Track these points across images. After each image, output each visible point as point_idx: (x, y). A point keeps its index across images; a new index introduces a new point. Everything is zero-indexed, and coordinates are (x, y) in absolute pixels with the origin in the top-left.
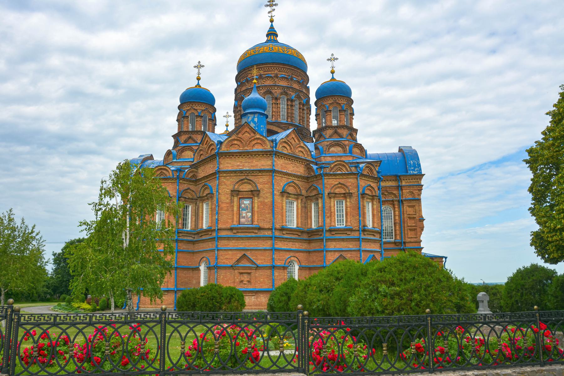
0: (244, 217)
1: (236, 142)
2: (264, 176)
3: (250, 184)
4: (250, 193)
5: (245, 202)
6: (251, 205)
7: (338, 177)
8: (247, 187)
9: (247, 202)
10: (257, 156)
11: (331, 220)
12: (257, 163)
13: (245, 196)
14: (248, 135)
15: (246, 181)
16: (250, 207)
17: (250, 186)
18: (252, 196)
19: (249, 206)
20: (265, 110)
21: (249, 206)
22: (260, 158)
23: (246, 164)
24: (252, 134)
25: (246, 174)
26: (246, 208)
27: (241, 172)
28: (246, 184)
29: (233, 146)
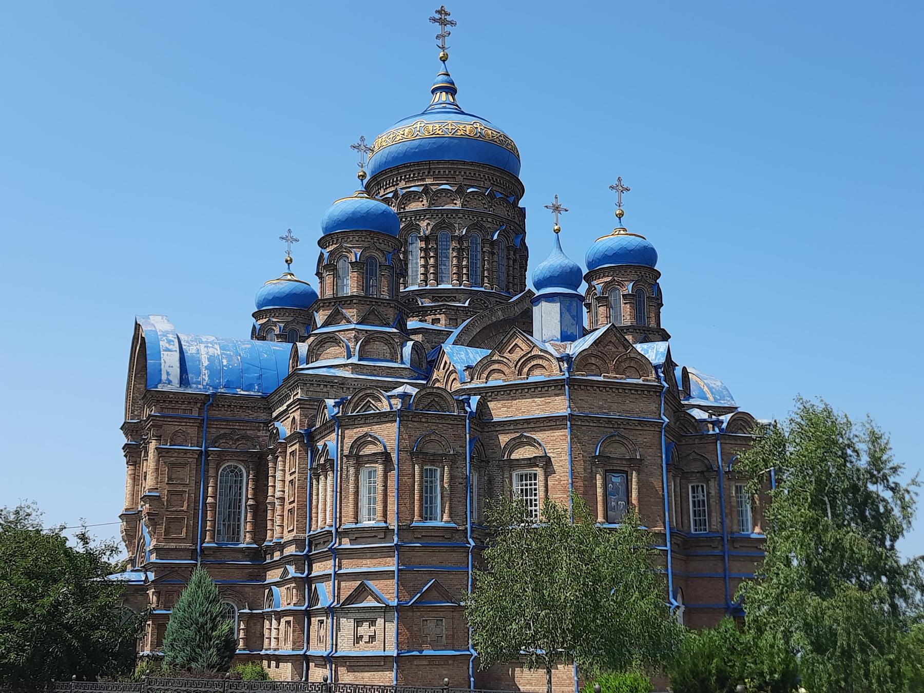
0: (613, 509)
1: (593, 360)
2: (644, 432)
3: (623, 444)
4: (624, 462)
5: (614, 479)
6: (624, 485)
7: (739, 442)
8: (617, 451)
9: (617, 479)
10: (633, 392)
11: (731, 521)
12: (631, 405)
13: (615, 468)
14: (613, 349)
15: (617, 438)
16: (622, 489)
17: (623, 448)
18: (626, 469)
19: (620, 487)
20: (576, 287)
21: (620, 487)
22: (637, 397)
23: (615, 406)
24: (621, 349)
25: (616, 426)
26: (616, 492)
27: (609, 420)
28: (615, 445)
29: (587, 367)
